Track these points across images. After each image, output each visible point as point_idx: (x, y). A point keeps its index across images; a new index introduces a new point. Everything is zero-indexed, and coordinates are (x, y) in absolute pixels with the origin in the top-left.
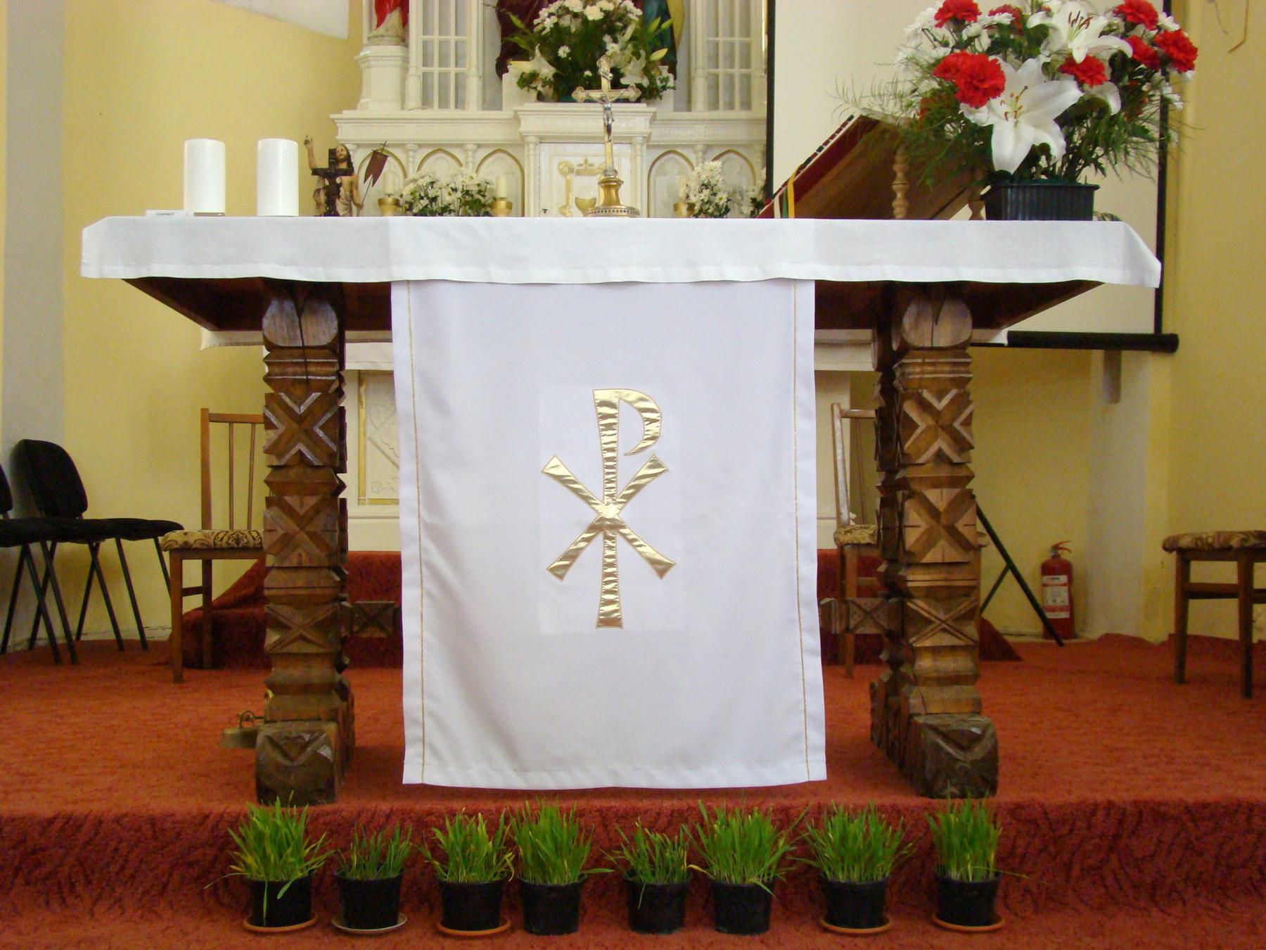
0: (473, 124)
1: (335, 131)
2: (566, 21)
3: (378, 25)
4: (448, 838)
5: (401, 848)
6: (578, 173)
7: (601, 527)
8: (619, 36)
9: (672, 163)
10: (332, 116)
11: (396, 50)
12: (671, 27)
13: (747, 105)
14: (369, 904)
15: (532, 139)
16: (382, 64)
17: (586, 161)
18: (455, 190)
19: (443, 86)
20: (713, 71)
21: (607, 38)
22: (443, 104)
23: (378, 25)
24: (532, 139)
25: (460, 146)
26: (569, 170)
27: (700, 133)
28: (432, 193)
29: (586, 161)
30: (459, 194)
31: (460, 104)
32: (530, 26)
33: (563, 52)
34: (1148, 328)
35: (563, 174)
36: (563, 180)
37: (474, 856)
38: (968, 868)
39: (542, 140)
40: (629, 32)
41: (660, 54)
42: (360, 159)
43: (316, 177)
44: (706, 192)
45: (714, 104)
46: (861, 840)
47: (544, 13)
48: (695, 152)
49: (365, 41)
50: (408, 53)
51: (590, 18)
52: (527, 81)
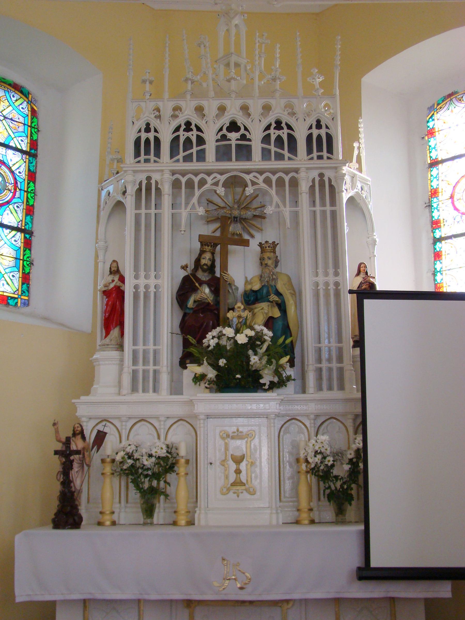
0: (162, 404)
1: (75, 410)
2: (223, 342)
3: (106, 337)
6: (233, 438)
8: (259, 350)
9: (294, 427)
10: (74, 401)
11: (115, 354)
12: (292, 342)
13: (341, 387)
15: (202, 417)
17: (238, 430)
18: (150, 456)
19: (145, 378)
20: (319, 365)
21: (250, 352)
23: (106, 337)
24: (202, 417)
25: (157, 418)
26: (226, 436)
27: (312, 408)
28: (136, 456)
29: (238, 430)
30: (153, 459)
33: (222, 362)
35: (223, 438)
36: (222, 442)
39: (208, 417)
40: (265, 347)
41: (284, 360)
42: (91, 436)
43: (57, 456)
44: (319, 457)
45: (320, 388)
47: (209, 335)
48: (309, 419)
49: (98, 347)
50: (123, 356)
51: (240, 342)
52: (198, 379)
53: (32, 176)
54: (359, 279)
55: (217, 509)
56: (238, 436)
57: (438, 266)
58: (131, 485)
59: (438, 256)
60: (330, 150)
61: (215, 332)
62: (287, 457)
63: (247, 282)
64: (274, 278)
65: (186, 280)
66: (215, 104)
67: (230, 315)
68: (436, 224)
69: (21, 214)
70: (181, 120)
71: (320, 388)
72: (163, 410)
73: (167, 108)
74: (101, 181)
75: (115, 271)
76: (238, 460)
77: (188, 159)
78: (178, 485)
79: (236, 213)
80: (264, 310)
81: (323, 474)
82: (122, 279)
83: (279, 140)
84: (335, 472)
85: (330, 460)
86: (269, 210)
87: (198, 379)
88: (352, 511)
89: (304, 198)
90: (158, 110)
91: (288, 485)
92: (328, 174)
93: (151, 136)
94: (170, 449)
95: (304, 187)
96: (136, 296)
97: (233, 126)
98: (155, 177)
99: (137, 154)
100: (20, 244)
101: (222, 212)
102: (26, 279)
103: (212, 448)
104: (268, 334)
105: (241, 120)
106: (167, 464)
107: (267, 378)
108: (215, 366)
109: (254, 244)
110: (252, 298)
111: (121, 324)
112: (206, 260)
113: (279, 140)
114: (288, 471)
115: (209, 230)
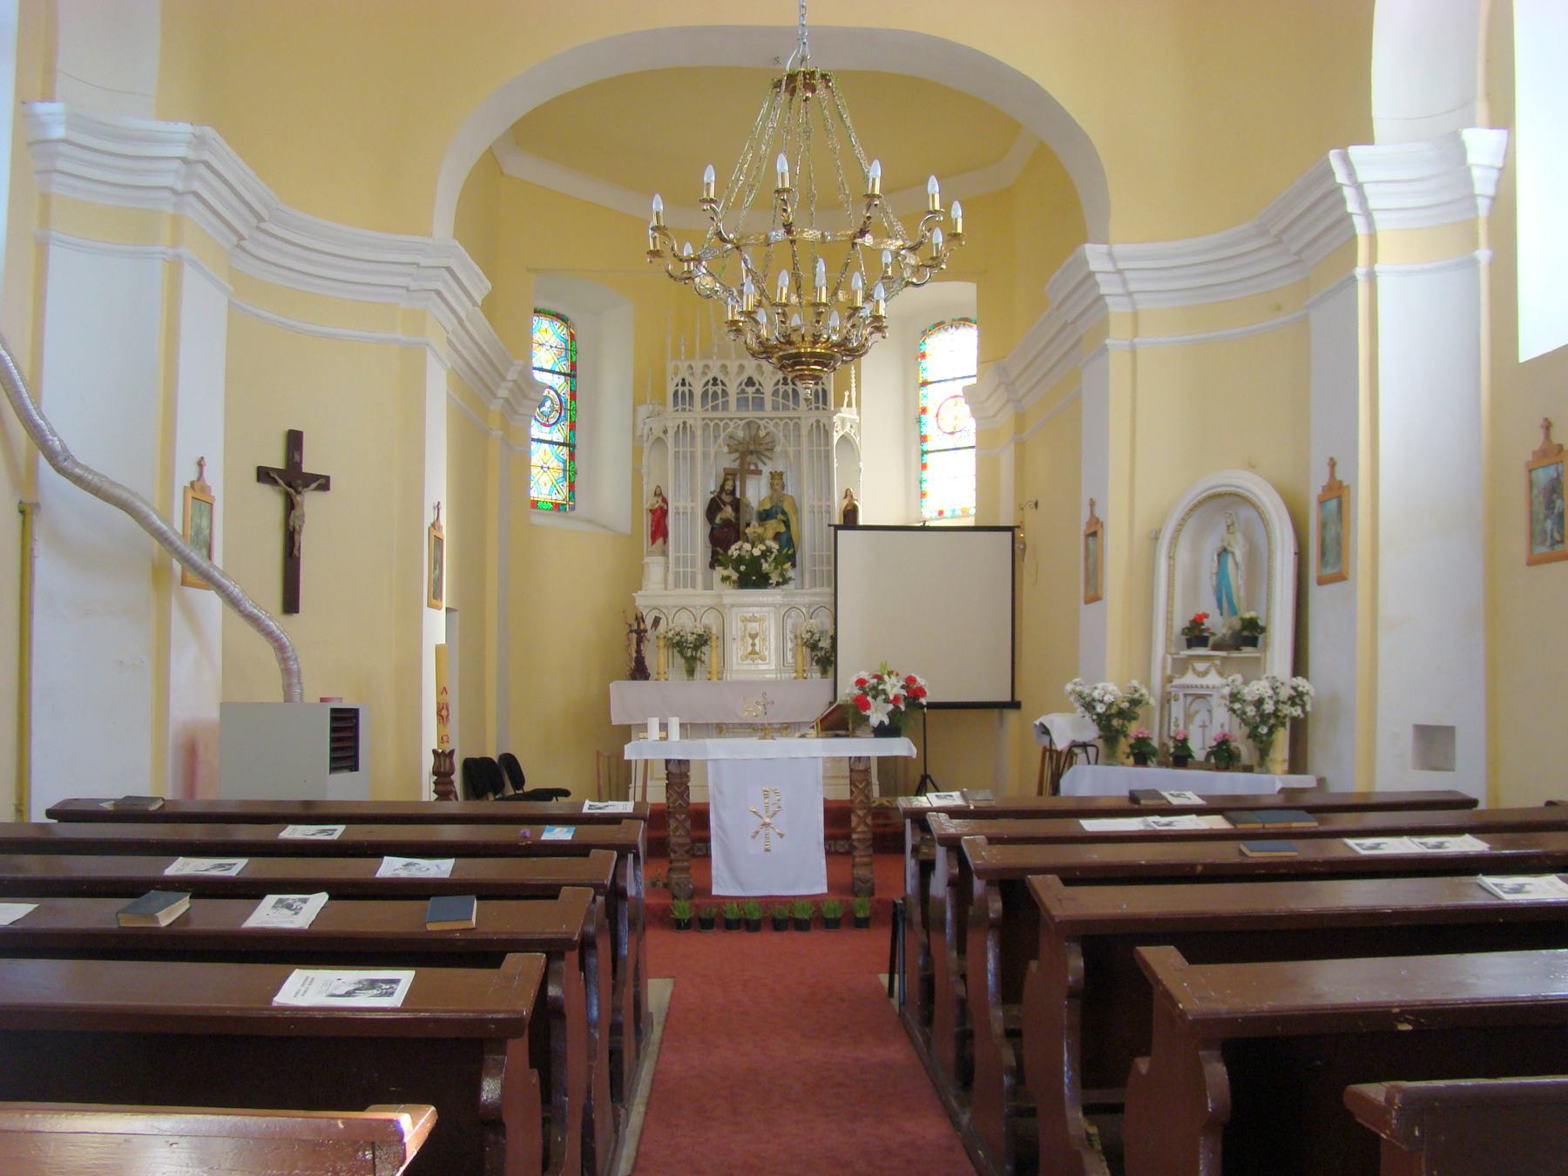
0: (699, 597)
4: (727, 907)
5: (714, 911)
7: (765, 825)
11: (661, 559)
14: (705, 924)
16: (655, 568)
22: (685, 587)
26: (745, 620)
27: (807, 600)
31: (694, 587)
32: (727, 548)
33: (742, 568)
34: (1008, 699)
37: (732, 913)
38: (860, 915)
41: (787, 566)
46: (832, 909)
53: (573, 395)
54: (845, 502)
55: (738, 665)
56: (754, 619)
57: (925, 474)
58: (677, 655)
59: (924, 466)
60: (825, 403)
61: (736, 546)
62: (789, 636)
63: (760, 503)
64: (782, 498)
65: (713, 500)
66: (737, 363)
67: (748, 530)
68: (923, 439)
69: (566, 429)
70: (710, 377)
72: (699, 601)
73: (698, 365)
74: (637, 402)
75: (659, 494)
76: (753, 637)
77: (715, 408)
78: (709, 654)
79: (752, 448)
80: (774, 526)
81: (814, 646)
82: (665, 501)
84: (821, 644)
85: (816, 637)
86: (778, 449)
87: (725, 579)
88: (831, 670)
89: (805, 441)
90: (691, 367)
91: (789, 655)
92: (823, 421)
93: (686, 389)
94: (707, 629)
95: (804, 432)
96: (677, 513)
97: (750, 382)
98: (690, 422)
99: (676, 404)
101: (741, 448)
102: (572, 487)
103: (735, 627)
104: (775, 546)
105: (756, 377)
106: (702, 640)
107: (774, 579)
108: (737, 569)
109: (766, 470)
110: (764, 516)
111: (665, 535)
112: (728, 487)
114: (790, 645)
115: (730, 462)
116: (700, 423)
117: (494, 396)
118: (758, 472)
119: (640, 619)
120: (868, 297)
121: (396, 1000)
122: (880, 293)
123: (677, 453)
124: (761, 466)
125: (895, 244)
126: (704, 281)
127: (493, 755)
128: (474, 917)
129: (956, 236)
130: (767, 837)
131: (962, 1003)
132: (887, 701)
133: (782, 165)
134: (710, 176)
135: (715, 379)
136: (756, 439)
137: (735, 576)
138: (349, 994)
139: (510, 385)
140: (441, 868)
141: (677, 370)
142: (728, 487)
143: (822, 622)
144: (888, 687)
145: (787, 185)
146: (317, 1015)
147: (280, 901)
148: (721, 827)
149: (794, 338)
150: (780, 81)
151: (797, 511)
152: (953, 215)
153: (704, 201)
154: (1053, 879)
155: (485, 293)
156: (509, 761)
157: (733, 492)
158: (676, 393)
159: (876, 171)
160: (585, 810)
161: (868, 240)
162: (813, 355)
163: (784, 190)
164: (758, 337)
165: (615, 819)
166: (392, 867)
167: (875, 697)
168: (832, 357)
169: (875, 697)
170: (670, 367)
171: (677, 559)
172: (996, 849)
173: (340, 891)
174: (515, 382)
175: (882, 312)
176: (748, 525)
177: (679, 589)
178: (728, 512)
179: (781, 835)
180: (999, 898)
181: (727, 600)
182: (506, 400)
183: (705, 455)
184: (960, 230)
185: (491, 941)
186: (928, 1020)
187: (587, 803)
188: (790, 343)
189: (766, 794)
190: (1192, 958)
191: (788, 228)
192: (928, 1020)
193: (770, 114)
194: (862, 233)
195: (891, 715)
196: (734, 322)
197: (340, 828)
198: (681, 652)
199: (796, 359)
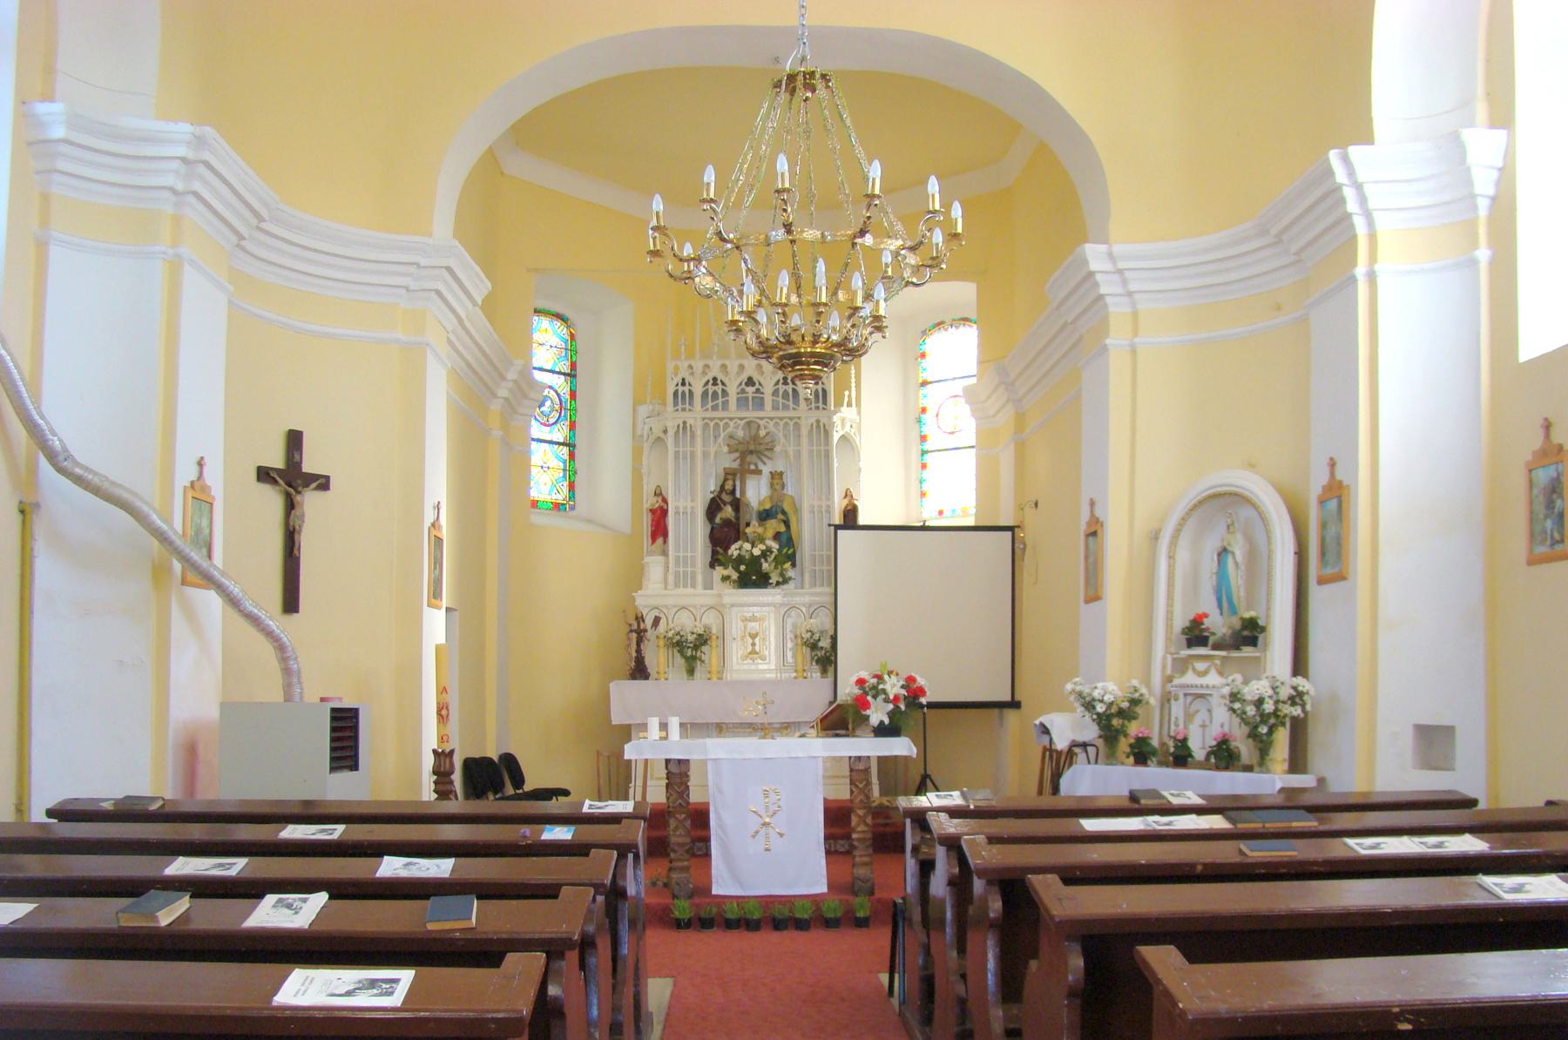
0: (698, 596)
4: (727, 907)
5: (714, 910)
7: (765, 824)
11: (661, 558)
14: (705, 923)
16: (655, 567)
26: (745, 620)
27: (807, 599)
31: (694, 586)
32: (727, 548)
33: (743, 568)
34: (1008, 698)
37: (732, 912)
38: (861, 914)
41: (787, 565)
46: (832, 908)
47: (733, 547)
53: (573, 395)
54: (846, 502)
55: (739, 665)
56: (754, 619)
59: (924, 466)
60: (825, 403)
62: (789, 635)
63: (760, 503)
64: (781, 498)
65: (713, 500)
66: (737, 363)
67: (748, 530)
69: (566, 430)
70: (710, 377)
71: (814, 585)
72: (699, 601)
73: (698, 365)
74: (637, 402)
75: (658, 493)
76: (754, 636)
77: (715, 408)
78: (710, 654)
79: (752, 447)
80: (774, 526)
81: (814, 646)
82: (665, 501)
83: (786, 394)
84: (821, 644)
85: (816, 637)
86: (778, 449)
87: (725, 579)
88: (831, 669)
89: (805, 440)
90: (691, 367)
91: (789, 654)
92: (824, 420)
93: (686, 389)
94: (707, 628)
95: (804, 431)
96: (677, 513)
97: (750, 382)
99: (676, 404)
100: (567, 457)
101: (741, 448)
102: (572, 486)
103: (735, 628)
104: (775, 546)
105: (756, 377)
106: (702, 640)
107: (774, 579)
108: (737, 569)
110: (765, 516)
111: (665, 535)
112: (728, 486)
113: (786, 392)
114: (790, 645)
115: (730, 462)
116: (700, 423)
117: (494, 395)
118: (759, 472)
119: (640, 619)
120: (868, 297)
121: (396, 1000)
122: (879, 292)
123: (677, 453)
124: (761, 466)
125: (895, 244)
126: (704, 281)
127: (493, 754)
128: (473, 917)
129: (956, 236)
130: (767, 836)
131: (962, 1002)
132: (887, 700)
133: (782, 164)
134: (710, 176)
135: (715, 379)
136: (755, 438)
137: (735, 576)
138: (349, 994)
139: (510, 384)
140: (439, 868)
141: (677, 368)
142: (728, 486)
143: (822, 622)
144: (888, 687)
145: (787, 185)
146: (318, 1014)
147: (280, 901)
148: (721, 826)
149: (794, 337)
150: (780, 81)
151: (797, 511)
152: (953, 215)
153: (704, 201)
154: (1053, 879)
155: (486, 293)
156: (509, 761)
157: (733, 492)
158: (676, 394)
159: (875, 171)
160: (585, 809)
161: (868, 240)
162: (813, 355)
163: (784, 190)
164: (758, 337)
165: (615, 819)
166: (392, 867)
167: (875, 697)
168: (832, 357)
169: (875, 697)
170: (670, 366)
171: (677, 559)
172: (995, 848)
173: (340, 891)
174: (515, 382)
175: (882, 312)
176: (748, 525)
177: (680, 589)
178: (728, 512)
179: (781, 835)
180: (998, 897)
181: (727, 600)
182: (506, 399)
183: (705, 455)
184: (960, 230)
185: (491, 940)
186: (927, 1020)
187: (587, 802)
188: (790, 343)
189: (766, 794)
190: (1192, 958)
191: (788, 228)
192: (927, 1020)
193: (770, 114)
194: (862, 233)
195: (891, 715)
196: (734, 322)
197: (340, 828)
198: (681, 652)
199: (796, 359)
